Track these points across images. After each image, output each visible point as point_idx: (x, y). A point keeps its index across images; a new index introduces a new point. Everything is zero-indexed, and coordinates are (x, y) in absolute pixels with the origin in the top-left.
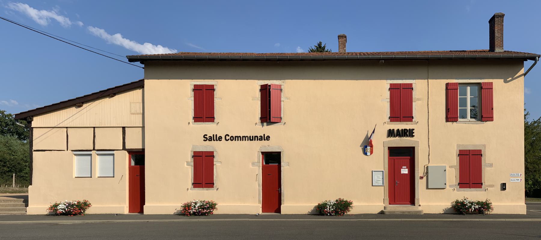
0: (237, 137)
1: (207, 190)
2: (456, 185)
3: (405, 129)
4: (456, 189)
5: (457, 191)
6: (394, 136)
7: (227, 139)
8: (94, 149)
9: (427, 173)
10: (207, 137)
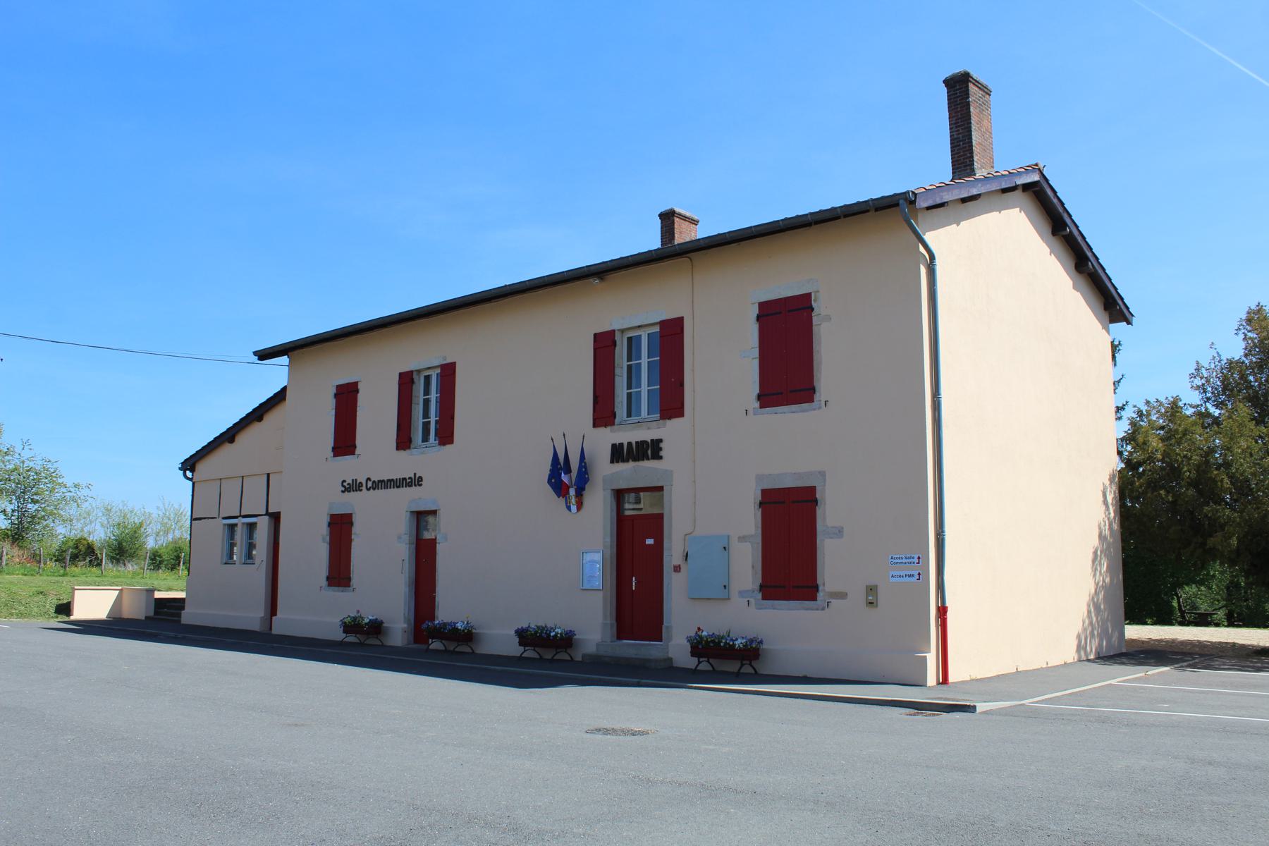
2: (754, 591)
3: (644, 442)
4: (752, 600)
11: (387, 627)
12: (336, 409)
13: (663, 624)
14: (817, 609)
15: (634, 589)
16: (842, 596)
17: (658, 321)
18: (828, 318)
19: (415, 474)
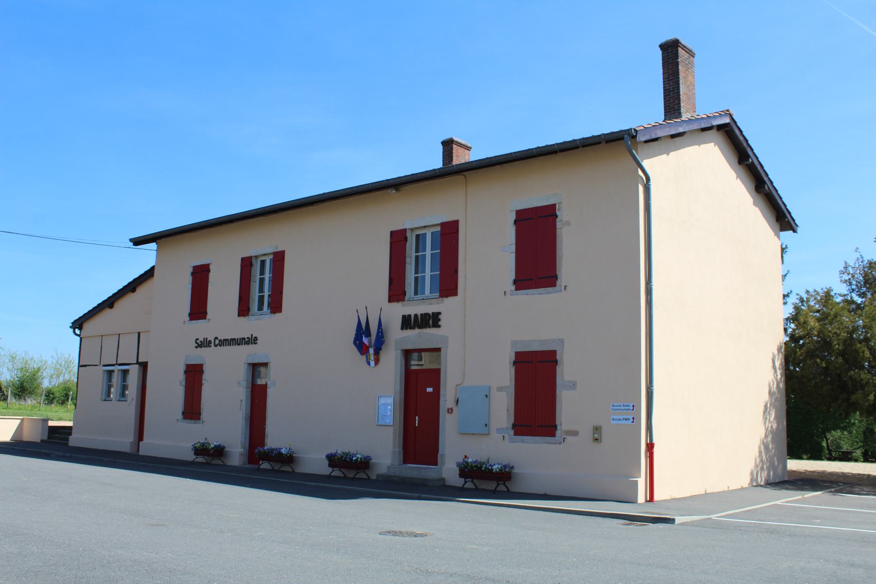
1: (194, 423)
2: (508, 429)
3: (427, 314)
4: (506, 436)
5: (510, 442)
6: (411, 328)
7: (216, 344)
11: (227, 451)
13: (438, 452)
14: (556, 443)
15: (417, 425)
16: (575, 433)
17: (440, 222)
18: (568, 223)
19: (252, 335)
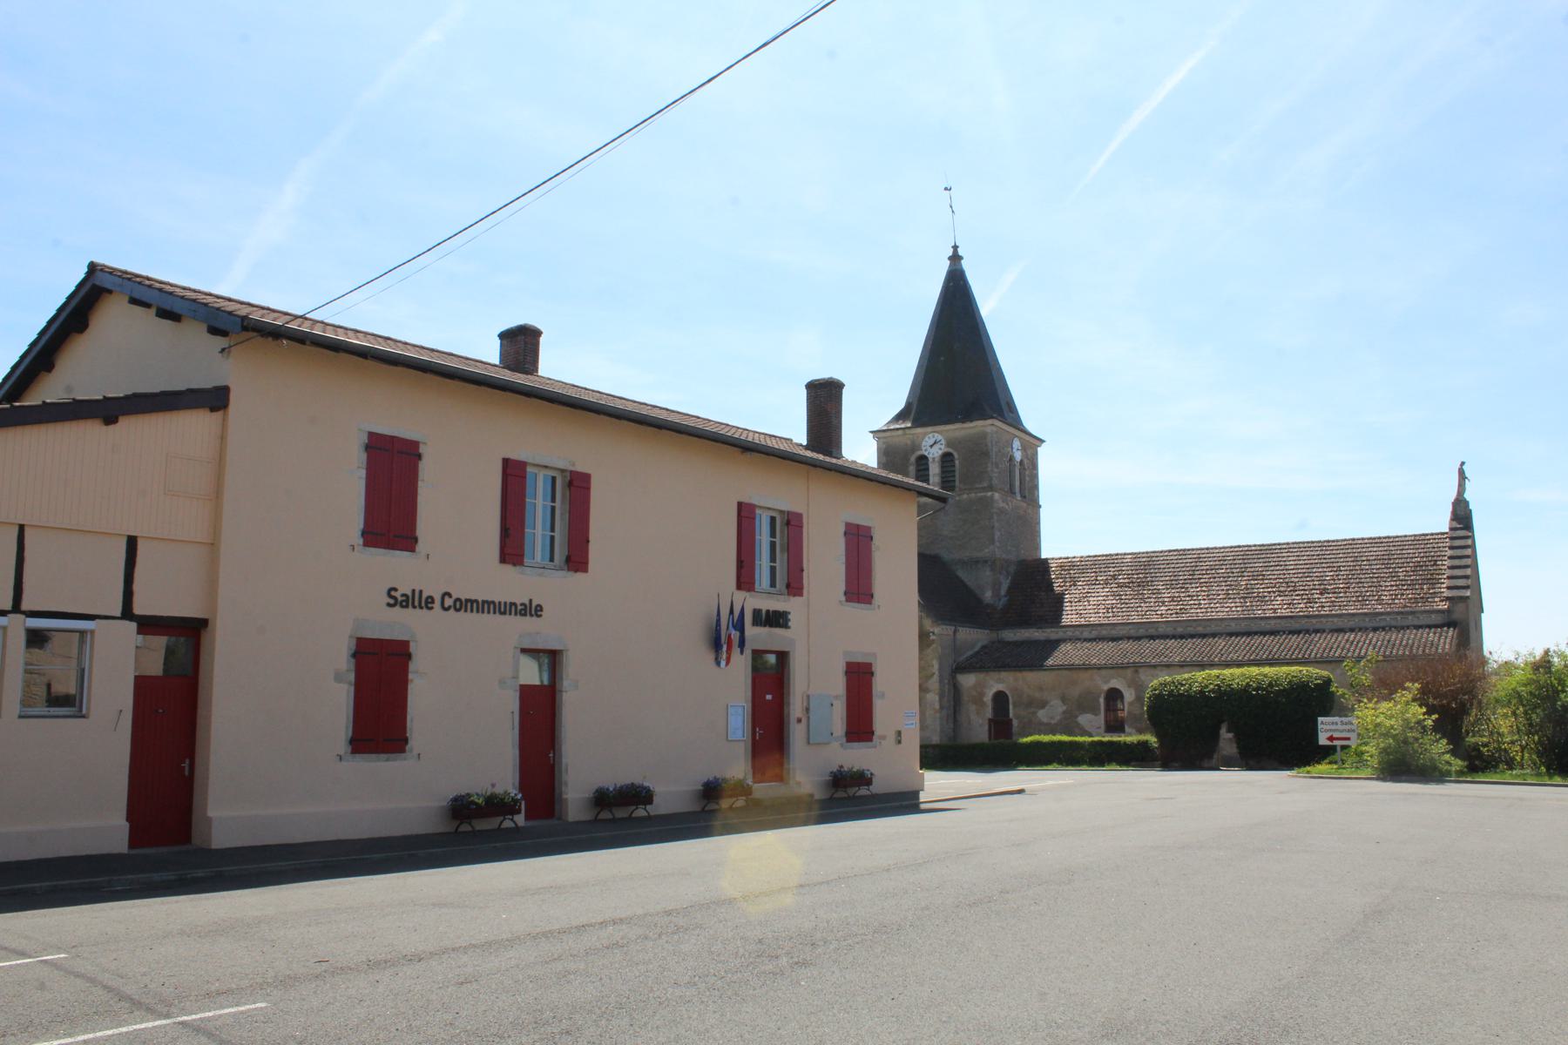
0: (487, 602)
1: (387, 760)
7: (446, 605)
8: (16, 608)
9: (807, 710)
10: (397, 594)
12: (367, 469)
19: (531, 601)
